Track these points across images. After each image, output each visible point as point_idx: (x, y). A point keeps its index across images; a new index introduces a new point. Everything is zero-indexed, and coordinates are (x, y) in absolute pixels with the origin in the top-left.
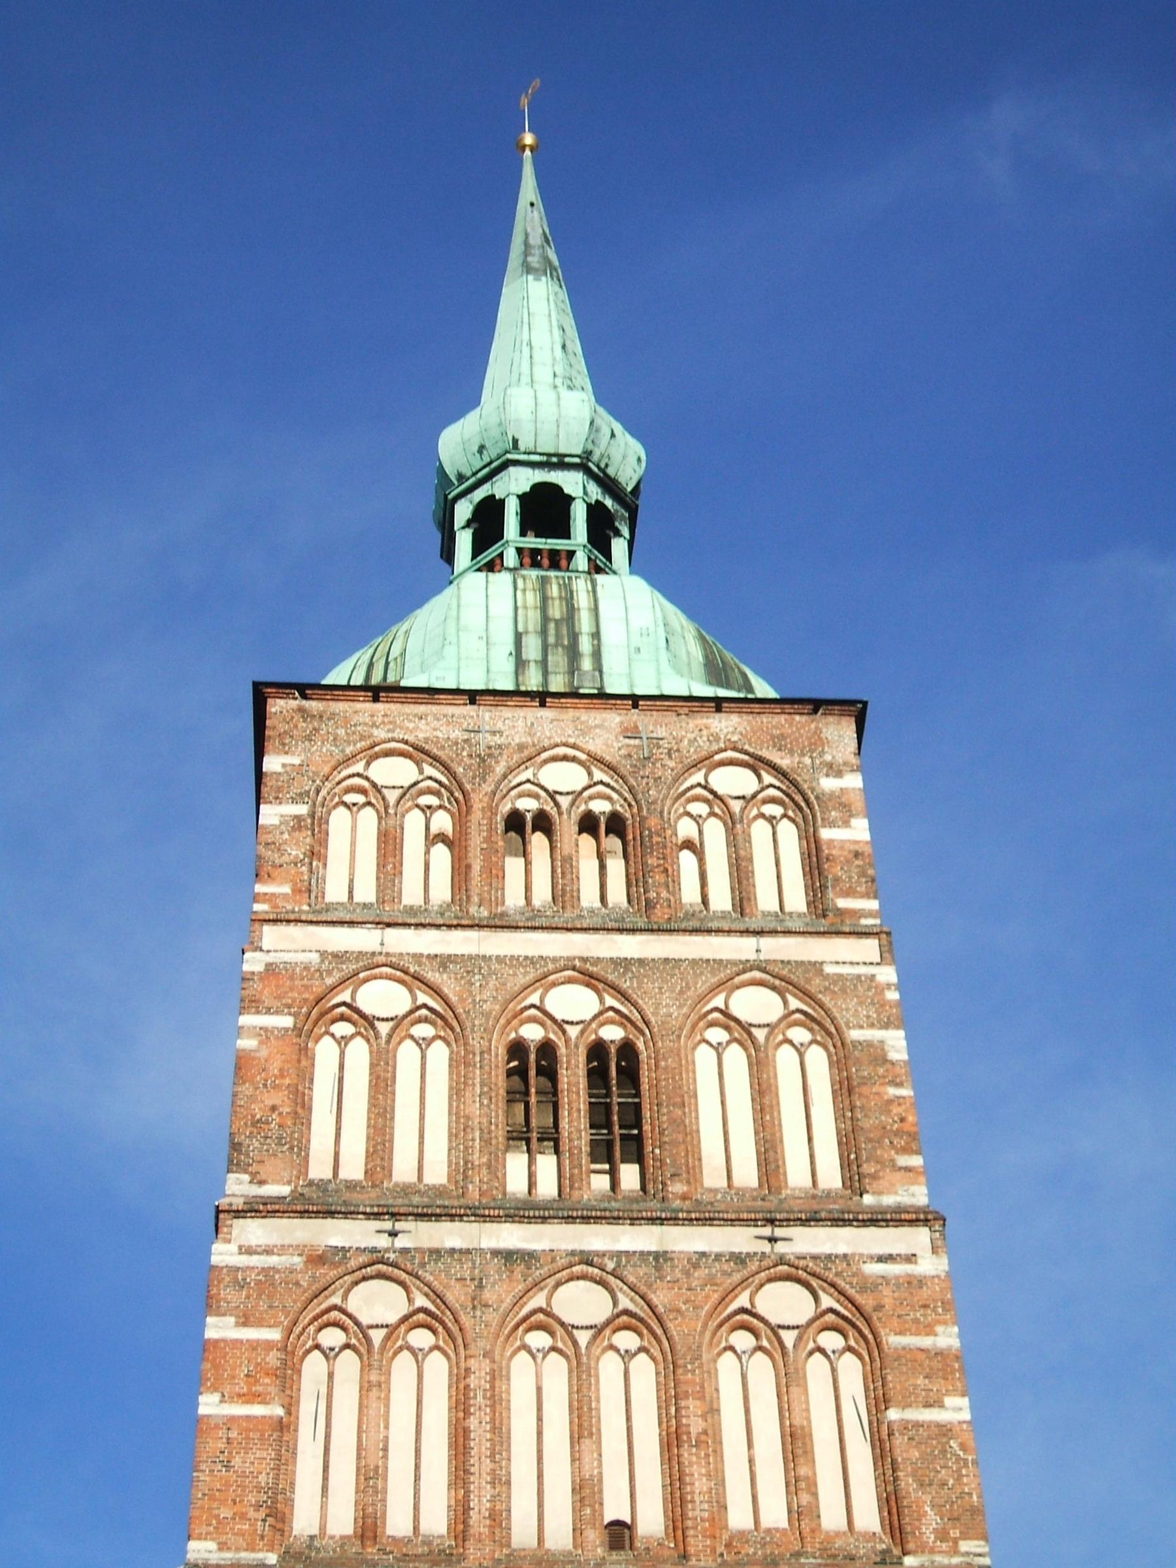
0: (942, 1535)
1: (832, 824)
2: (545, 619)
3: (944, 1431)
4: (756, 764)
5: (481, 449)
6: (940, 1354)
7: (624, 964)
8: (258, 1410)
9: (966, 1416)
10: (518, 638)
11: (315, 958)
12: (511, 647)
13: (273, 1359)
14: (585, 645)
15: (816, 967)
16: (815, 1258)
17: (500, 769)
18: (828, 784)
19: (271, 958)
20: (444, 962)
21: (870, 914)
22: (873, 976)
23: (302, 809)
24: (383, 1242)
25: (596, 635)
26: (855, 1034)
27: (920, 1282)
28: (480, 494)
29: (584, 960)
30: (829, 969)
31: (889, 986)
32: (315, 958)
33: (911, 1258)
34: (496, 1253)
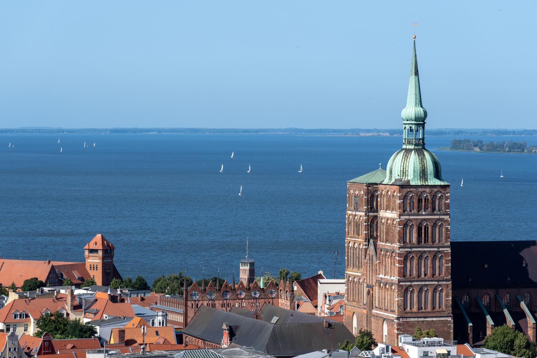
0: (448, 276)
1: (446, 200)
2: (423, 170)
3: (449, 266)
4: (441, 192)
5: (411, 119)
6: (450, 259)
7: (429, 219)
8: (402, 266)
9: (450, 265)
10: (420, 173)
11: (404, 219)
12: (419, 175)
13: (403, 261)
14: (426, 175)
15: (444, 218)
16: (441, 251)
17: (419, 194)
18: (447, 195)
19: (401, 219)
20: (414, 219)
21: (448, 211)
22: (448, 220)
23: (402, 201)
24: (410, 250)
25: (427, 172)
26: (446, 226)
27: (449, 253)
28: (410, 125)
29: (425, 218)
30: (445, 219)
31: (450, 221)
32: (404, 219)
33: (448, 250)
34: (418, 251)
